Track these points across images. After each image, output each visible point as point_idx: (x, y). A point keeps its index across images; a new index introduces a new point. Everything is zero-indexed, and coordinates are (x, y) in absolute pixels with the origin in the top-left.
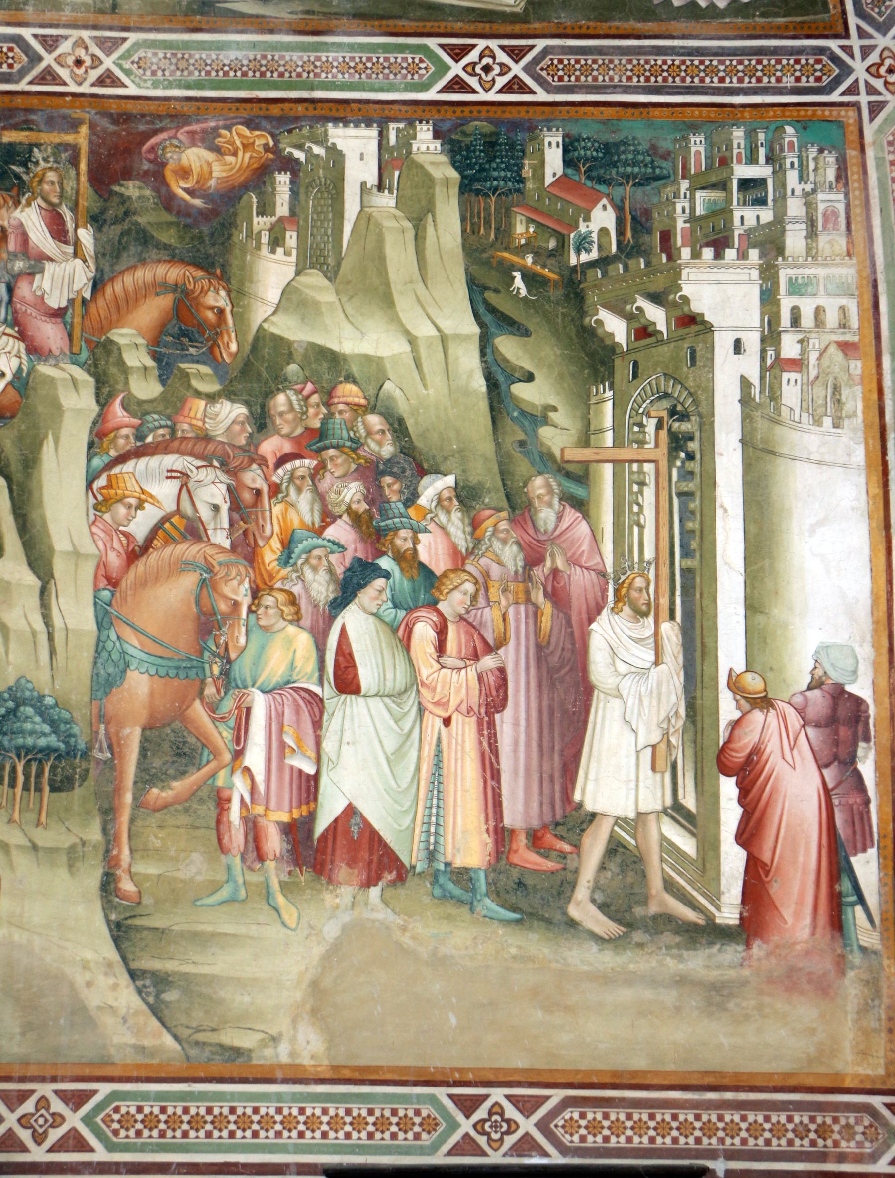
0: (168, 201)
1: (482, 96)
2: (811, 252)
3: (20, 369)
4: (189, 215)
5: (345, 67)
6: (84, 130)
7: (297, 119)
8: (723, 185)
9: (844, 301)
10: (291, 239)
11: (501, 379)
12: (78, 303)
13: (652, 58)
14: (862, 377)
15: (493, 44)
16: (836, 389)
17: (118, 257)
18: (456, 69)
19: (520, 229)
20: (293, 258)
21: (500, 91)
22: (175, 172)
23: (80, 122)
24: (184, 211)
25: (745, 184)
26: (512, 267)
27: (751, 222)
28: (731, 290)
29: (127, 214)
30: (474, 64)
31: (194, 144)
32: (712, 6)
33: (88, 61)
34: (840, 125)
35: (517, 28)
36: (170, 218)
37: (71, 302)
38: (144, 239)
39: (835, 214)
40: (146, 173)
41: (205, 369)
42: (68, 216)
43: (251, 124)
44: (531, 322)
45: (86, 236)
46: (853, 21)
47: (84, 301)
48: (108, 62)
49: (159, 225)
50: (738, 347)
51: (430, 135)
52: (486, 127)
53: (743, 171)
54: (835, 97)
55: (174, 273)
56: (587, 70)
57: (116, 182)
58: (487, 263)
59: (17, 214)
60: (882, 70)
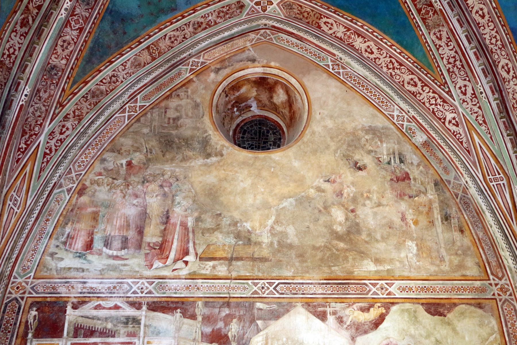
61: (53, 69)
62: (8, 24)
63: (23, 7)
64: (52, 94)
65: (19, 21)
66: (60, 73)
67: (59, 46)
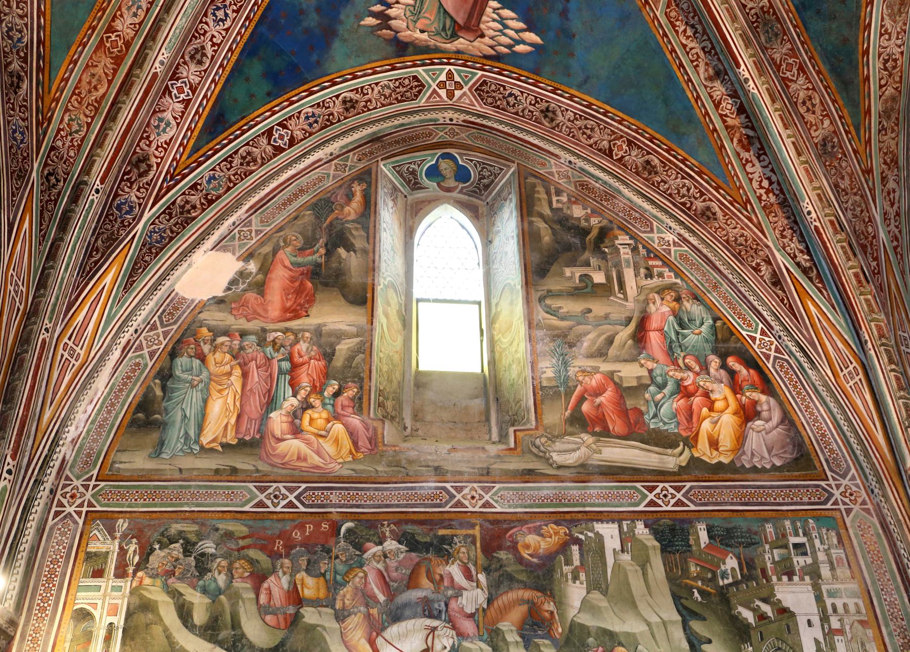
0: (520, 560)
1: (665, 508)
2: (834, 577)
3: (454, 644)
4: (532, 566)
5: (599, 496)
6: (478, 528)
7: (579, 520)
8: (786, 546)
9: (856, 600)
10: (583, 576)
11: (696, 643)
12: (481, 610)
13: (741, 490)
14: (874, 638)
15: (667, 485)
16: (863, 644)
17: (499, 587)
18: (651, 496)
19: (693, 569)
20: (585, 585)
21: (673, 506)
22: (523, 546)
23: (475, 525)
24: (528, 564)
25: (796, 546)
26: (692, 587)
27: (802, 563)
28: (800, 596)
29: (501, 566)
30: (659, 494)
31: (530, 533)
32: (763, 467)
33: (477, 497)
34: (834, 518)
35: (676, 478)
36: (523, 568)
37: (477, 610)
38: (511, 578)
39: (841, 559)
40: (509, 547)
41: (547, 642)
42: (472, 568)
43: (557, 523)
44: (706, 614)
45: (482, 577)
46: (829, 474)
47: (484, 609)
48: (487, 497)
49: (517, 571)
50: (809, 623)
51: (643, 526)
52: (669, 522)
53: (793, 540)
54: (828, 506)
55: (527, 594)
56: (712, 496)
57: (494, 551)
58: (679, 585)
59: (447, 568)
60: (847, 494)
61: (824, 145)
62: (730, 166)
63: (723, 133)
64: (850, 172)
65: (739, 149)
66: (835, 140)
67: (804, 115)
